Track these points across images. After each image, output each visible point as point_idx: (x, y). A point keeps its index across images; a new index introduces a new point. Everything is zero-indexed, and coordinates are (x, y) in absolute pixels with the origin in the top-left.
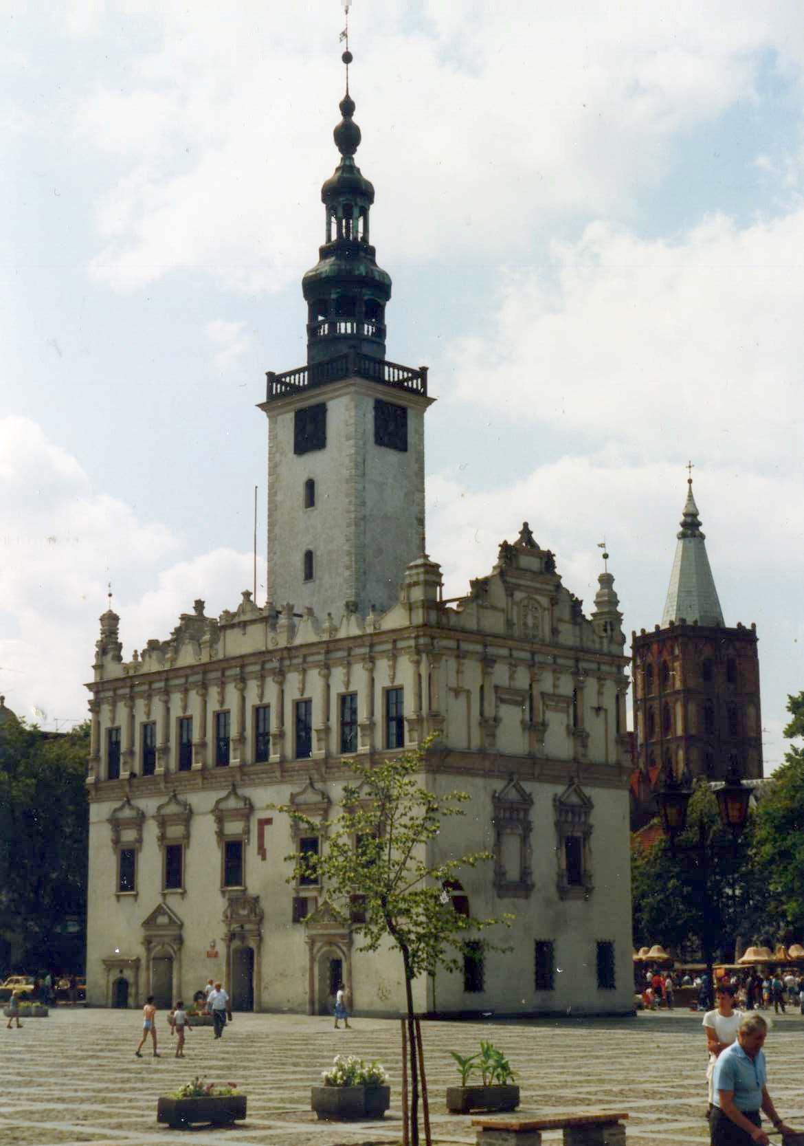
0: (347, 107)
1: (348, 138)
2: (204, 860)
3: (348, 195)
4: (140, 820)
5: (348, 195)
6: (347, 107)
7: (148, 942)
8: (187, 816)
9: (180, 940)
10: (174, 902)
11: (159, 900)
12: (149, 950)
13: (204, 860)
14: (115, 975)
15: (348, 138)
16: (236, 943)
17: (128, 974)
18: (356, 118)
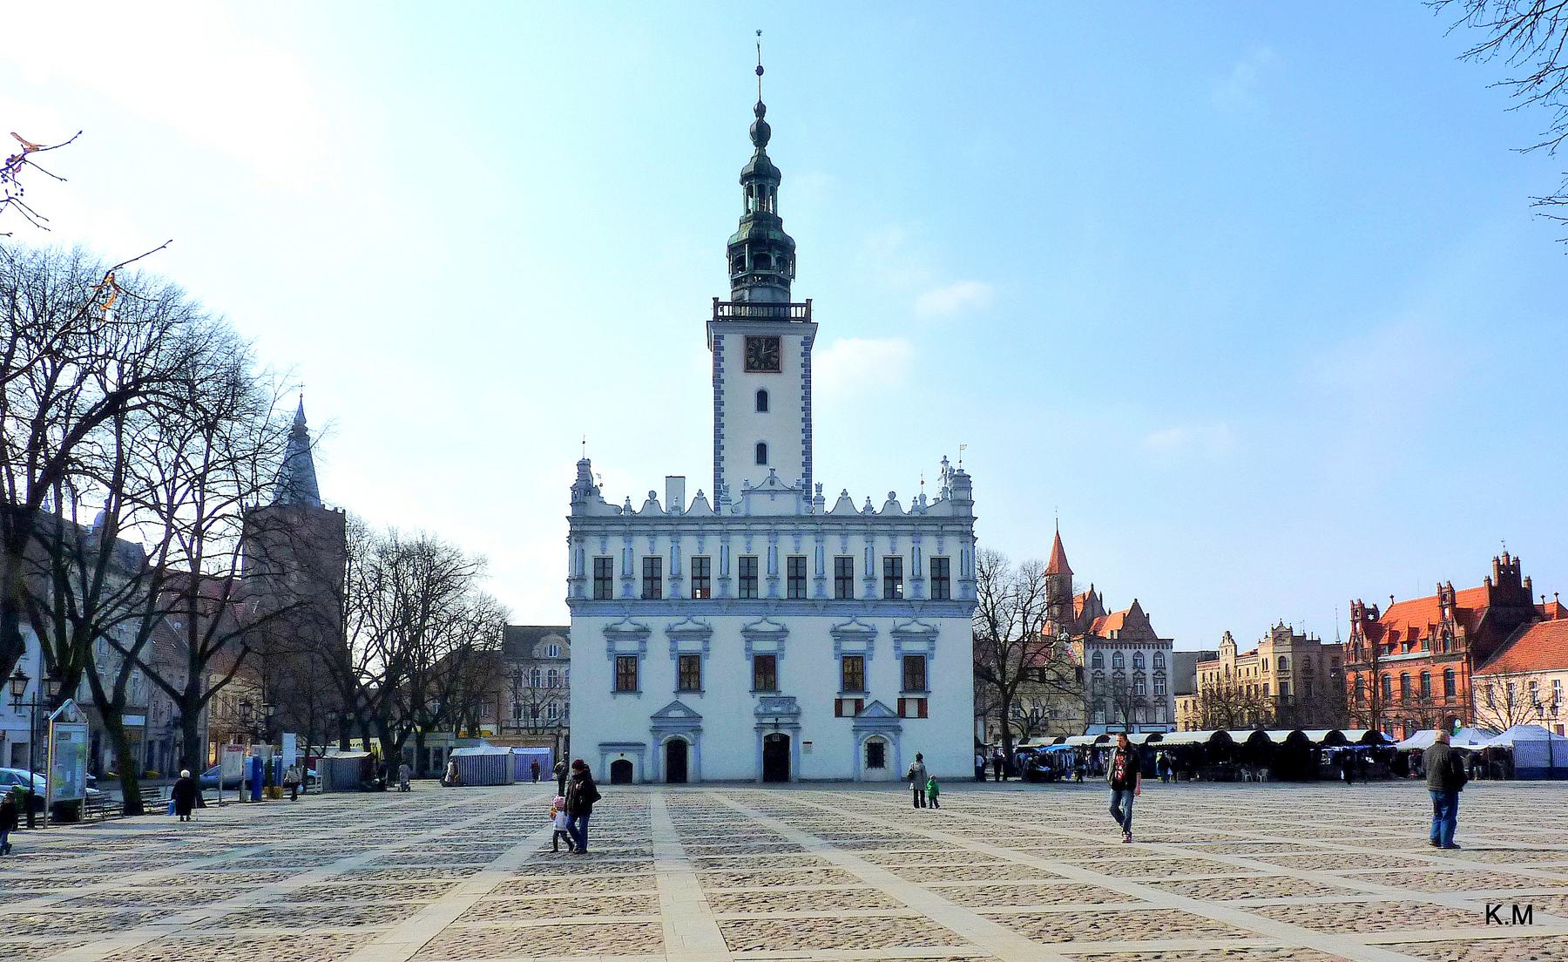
0: (760, 110)
1: (761, 134)
2: (728, 668)
3: (762, 179)
4: (642, 634)
5: (761, 179)
6: (760, 110)
7: (655, 730)
8: (705, 634)
9: (698, 730)
10: (689, 700)
11: (673, 698)
12: (657, 739)
13: (728, 668)
14: (614, 757)
15: (761, 134)
16: (770, 732)
17: (630, 757)
18: (766, 119)
